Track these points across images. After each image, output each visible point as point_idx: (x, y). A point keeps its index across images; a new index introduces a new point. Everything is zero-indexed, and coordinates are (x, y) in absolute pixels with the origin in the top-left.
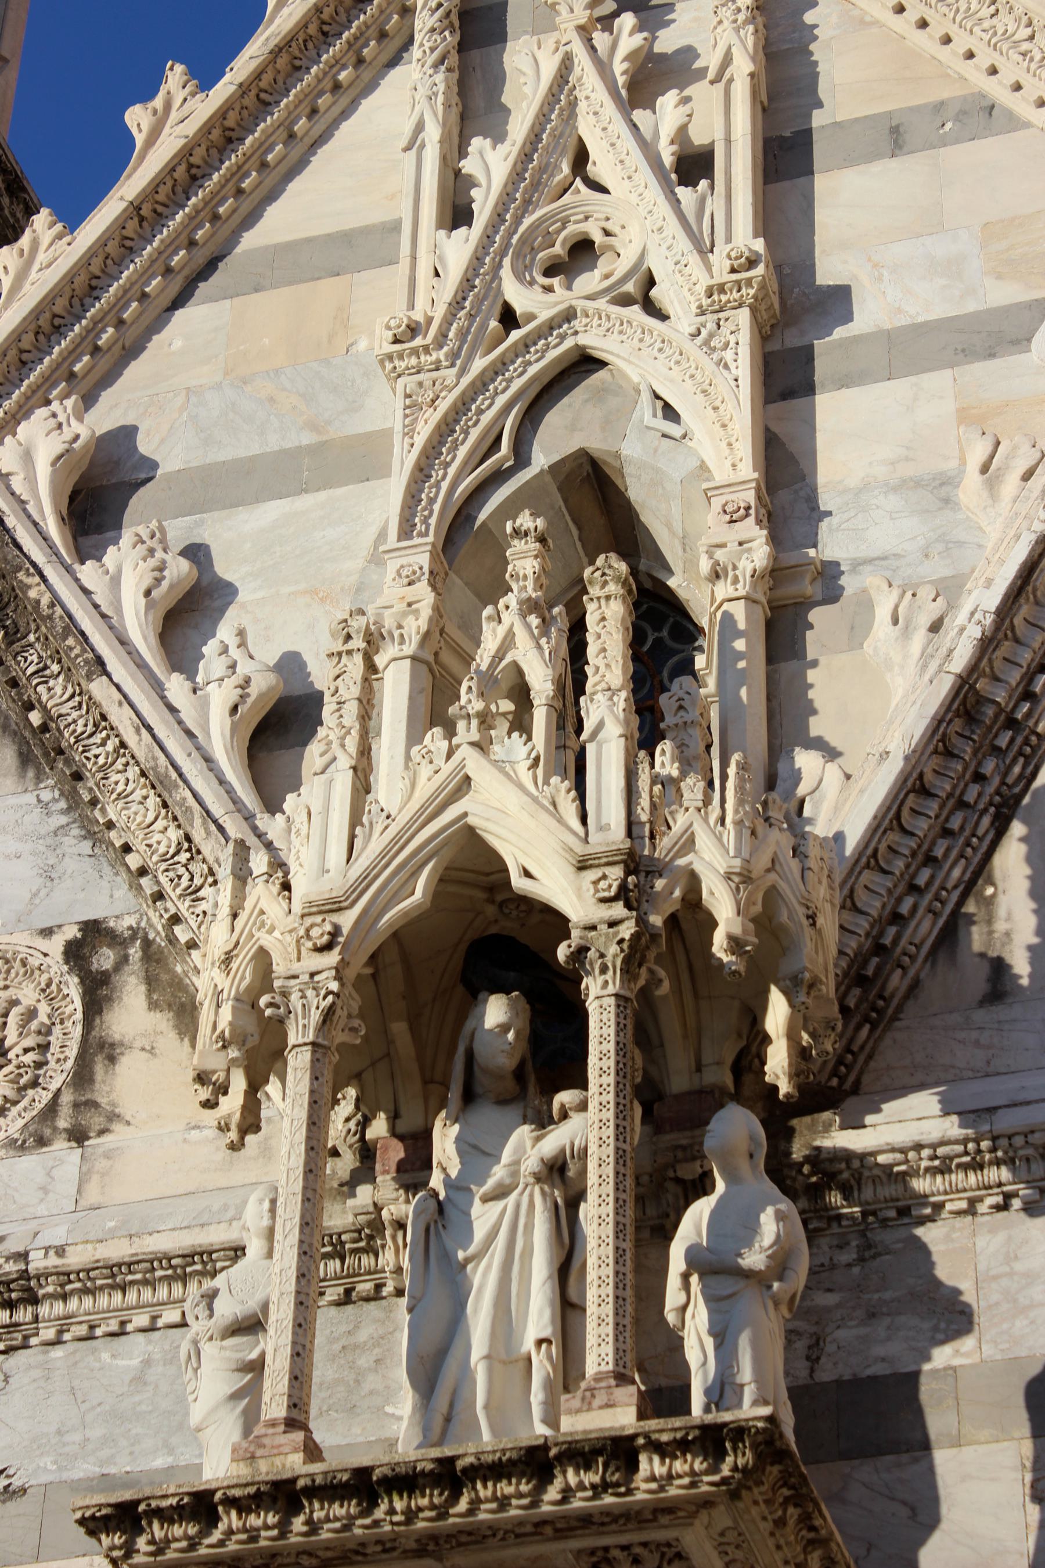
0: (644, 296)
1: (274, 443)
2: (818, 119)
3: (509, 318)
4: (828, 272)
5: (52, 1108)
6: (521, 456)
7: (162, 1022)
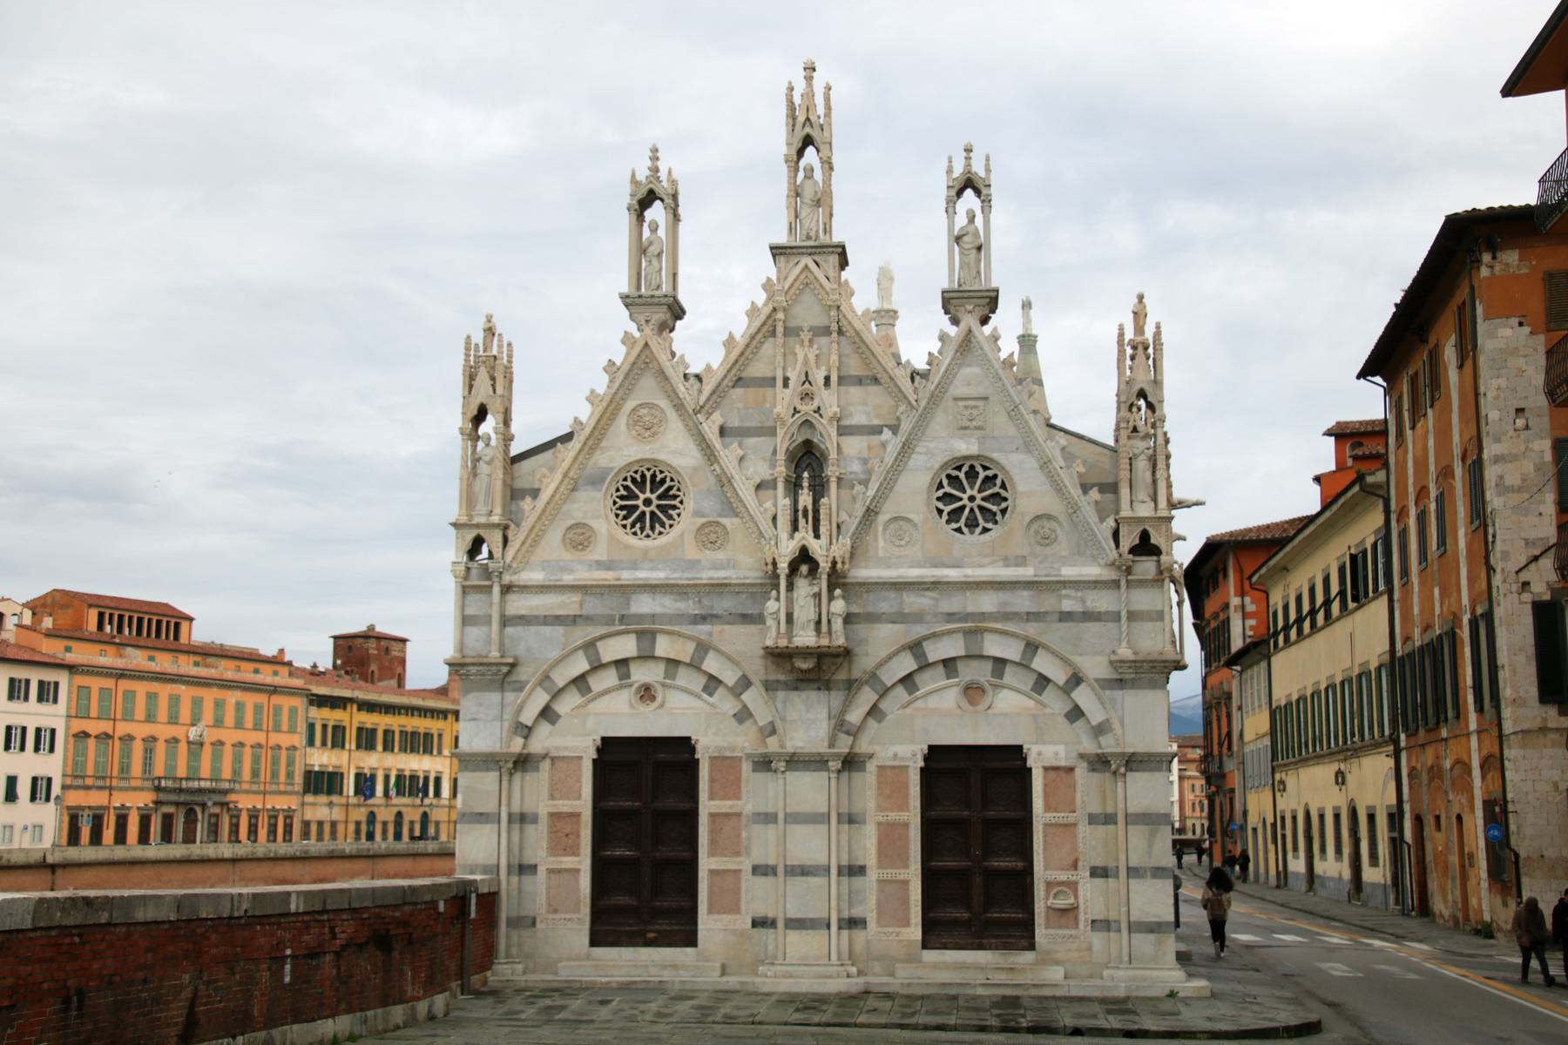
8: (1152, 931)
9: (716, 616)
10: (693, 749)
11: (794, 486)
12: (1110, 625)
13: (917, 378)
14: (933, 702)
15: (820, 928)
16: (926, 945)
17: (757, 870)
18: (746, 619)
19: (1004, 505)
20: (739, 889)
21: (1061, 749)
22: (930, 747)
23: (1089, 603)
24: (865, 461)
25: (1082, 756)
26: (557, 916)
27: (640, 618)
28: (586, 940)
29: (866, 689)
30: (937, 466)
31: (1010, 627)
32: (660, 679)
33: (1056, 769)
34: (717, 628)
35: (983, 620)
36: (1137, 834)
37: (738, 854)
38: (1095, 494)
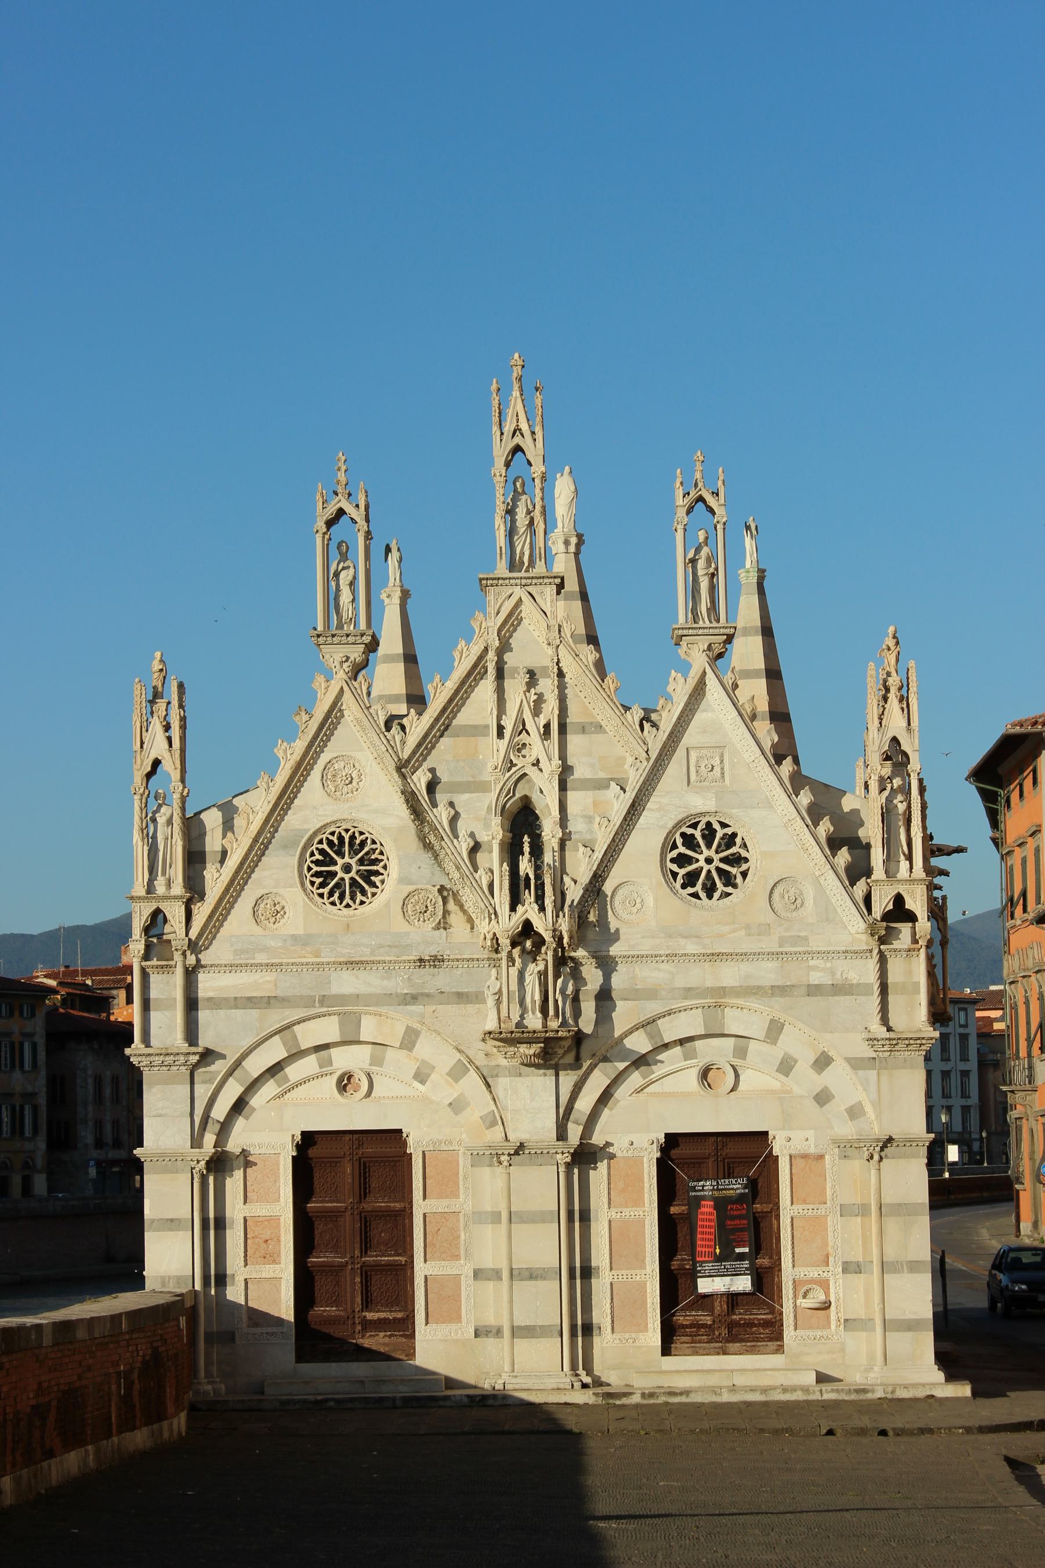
0: (537, 763)
1: (465, 779)
5: (439, 922)
7: (457, 908)
8: (909, 1329)
9: (428, 995)
10: (405, 1144)
11: (512, 852)
12: (863, 998)
13: (646, 725)
14: (668, 1085)
15: (552, 1336)
16: (666, 1351)
17: (477, 1274)
18: (461, 997)
19: (744, 867)
20: (459, 1296)
22: (667, 1135)
23: (838, 976)
24: (590, 819)
25: (834, 1141)
26: (258, 1330)
27: (342, 999)
28: (292, 1356)
29: (596, 1072)
31: (753, 1003)
32: (366, 1066)
33: (805, 1156)
34: (430, 1008)
35: (724, 996)
36: (892, 1225)
37: (457, 1257)
38: (844, 856)
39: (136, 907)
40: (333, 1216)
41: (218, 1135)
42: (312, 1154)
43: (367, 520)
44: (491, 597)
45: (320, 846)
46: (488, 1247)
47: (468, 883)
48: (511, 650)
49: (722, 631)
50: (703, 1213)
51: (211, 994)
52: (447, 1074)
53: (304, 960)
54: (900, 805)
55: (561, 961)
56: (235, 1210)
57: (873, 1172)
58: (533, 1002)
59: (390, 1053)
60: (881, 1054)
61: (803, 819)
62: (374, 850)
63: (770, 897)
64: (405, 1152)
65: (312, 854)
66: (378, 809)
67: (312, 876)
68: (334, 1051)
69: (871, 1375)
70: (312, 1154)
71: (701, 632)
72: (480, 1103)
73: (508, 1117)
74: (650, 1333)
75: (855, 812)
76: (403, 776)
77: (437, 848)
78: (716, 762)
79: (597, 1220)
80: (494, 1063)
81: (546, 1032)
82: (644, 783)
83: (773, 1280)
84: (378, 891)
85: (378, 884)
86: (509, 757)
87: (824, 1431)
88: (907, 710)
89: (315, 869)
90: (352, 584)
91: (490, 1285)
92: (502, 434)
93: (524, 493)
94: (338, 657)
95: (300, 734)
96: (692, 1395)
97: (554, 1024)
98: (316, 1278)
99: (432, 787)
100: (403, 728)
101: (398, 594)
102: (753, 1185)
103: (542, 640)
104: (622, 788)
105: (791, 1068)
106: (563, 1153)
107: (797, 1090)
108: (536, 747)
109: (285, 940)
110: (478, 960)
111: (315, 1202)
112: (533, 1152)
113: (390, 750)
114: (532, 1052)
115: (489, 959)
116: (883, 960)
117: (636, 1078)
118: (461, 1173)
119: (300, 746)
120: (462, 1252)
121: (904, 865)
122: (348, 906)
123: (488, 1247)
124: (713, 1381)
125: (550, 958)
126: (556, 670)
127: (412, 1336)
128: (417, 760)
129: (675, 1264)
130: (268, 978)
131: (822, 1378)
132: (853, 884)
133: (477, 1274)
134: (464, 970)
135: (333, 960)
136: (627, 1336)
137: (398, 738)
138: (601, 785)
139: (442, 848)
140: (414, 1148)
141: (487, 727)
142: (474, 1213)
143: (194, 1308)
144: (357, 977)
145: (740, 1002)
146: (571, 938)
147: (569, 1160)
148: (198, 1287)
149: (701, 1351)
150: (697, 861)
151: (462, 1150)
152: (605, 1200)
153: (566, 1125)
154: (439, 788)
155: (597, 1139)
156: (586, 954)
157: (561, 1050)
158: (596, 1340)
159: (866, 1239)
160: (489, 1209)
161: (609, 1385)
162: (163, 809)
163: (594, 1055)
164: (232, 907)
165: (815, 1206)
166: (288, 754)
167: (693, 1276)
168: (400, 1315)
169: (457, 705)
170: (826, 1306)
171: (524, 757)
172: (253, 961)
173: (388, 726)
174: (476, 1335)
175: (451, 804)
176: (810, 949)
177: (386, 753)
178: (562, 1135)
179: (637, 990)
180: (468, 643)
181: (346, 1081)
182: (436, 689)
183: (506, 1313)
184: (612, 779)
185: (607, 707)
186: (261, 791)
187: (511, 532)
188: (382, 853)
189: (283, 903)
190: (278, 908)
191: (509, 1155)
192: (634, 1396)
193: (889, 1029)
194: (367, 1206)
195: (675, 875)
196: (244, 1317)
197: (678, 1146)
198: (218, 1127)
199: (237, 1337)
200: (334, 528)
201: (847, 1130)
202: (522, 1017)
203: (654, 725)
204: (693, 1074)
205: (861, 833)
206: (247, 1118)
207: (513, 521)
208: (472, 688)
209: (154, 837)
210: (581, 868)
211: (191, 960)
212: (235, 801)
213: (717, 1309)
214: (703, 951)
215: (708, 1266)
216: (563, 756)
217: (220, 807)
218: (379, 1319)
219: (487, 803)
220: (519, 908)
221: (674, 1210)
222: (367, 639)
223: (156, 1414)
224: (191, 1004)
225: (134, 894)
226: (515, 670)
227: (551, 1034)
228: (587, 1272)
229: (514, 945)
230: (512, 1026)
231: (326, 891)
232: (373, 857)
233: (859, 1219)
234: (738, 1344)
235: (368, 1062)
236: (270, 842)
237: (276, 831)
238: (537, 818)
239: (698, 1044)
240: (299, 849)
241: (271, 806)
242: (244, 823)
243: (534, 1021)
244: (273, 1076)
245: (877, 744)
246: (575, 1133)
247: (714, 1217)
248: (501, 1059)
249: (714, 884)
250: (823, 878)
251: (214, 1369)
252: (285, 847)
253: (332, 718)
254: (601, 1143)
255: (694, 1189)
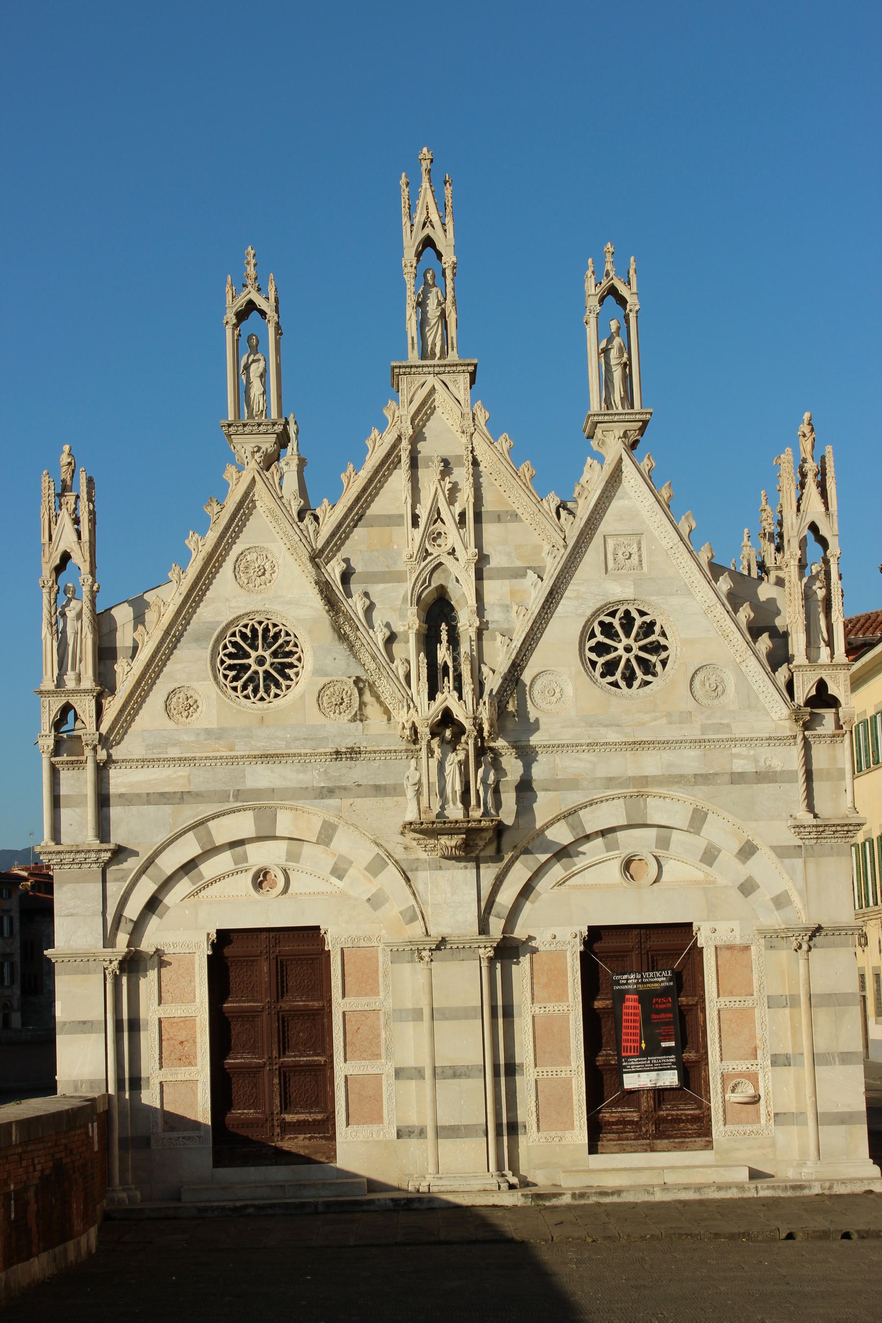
0: (452, 552)
2: (483, 509)
3: (427, 550)
4: (485, 552)
5: (356, 714)
6: (430, 584)
7: (373, 699)
8: (842, 1122)
9: (345, 788)
10: (323, 940)
11: (428, 642)
12: (786, 786)
13: (563, 513)
14: (589, 877)
15: (477, 1136)
16: (593, 1149)
17: (399, 1073)
18: (379, 790)
20: (381, 1095)
21: (735, 925)
22: (590, 928)
23: (762, 764)
24: (507, 608)
25: (760, 932)
26: (175, 1135)
27: (257, 793)
28: (210, 1161)
29: (518, 865)
30: (589, 613)
31: (676, 792)
32: (282, 862)
33: (730, 948)
34: (347, 802)
35: (646, 785)
36: (822, 1016)
37: (377, 1056)
38: (765, 643)
39: (45, 701)
40: (249, 1016)
41: (132, 934)
42: (229, 952)
43: (277, 311)
44: (403, 386)
45: (233, 639)
46: (410, 1045)
47: (385, 673)
48: (425, 439)
49: (638, 417)
50: (628, 1007)
51: (122, 790)
52: (366, 869)
53: (218, 754)
54: (819, 592)
55: (481, 751)
56: (150, 1011)
57: (802, 962)
58: (454, 792)
59: (307, 849)
60: (807, 842)
61: (723, 605)
62: (288, 643)
63: (691, 685)
64: (323, 949)
65: (225, 647)
66: (291, 599)
67: (225, 669)
68: (249, 847)
69: (805, 1170)
70: (229, 952)
71: (616, 418)
72: (399, 898)
73: (429, 911)
74: (577, 1131)
75: (772, 601)
76: (317, 566)
77: (352, 638)
78: (634, 549)
79: (520, 1015)
80: (413, 856)
81: (469, 822)
82: (562, 571)
83: (700, 1074)
84: (293, 683)
85: (293, 676)
86: (424, 546)
87: (784, 1235)
88: (824, 494)
89: (229, 662)
90: (263, 376)
91: (413, 1084)
92: (412, 225)
93: (434, 285)
94: (249, 448)
95: (212, 525)
96: (624, 1194)
97: (476, 814)
98: (233, 1080)
99: (346, 577)
100: (316, 518)
101: (296, 461)
102: (677, 977)
103: (456, 428)
104: (539, 577)
105: (715, 858)
106: (485, 947)
107: (721, 881)
108: (452, 535)
109: (198, 734)
110: (395, 751)
111: (232, 1002)
112: (455, 946)
113: (304, 540)
114: (453, 843)
115: (407, 751)
116: (807, 746)
117: (557, 871)
118: (381, 970)
119: (212, 536)
120: (383, 1051)
121: (825, 651)
122: (262, 699)
123: (410, 1045)
124: (644, 1179)
125: (471, 748)
126: (470, 458)
127: (333, 1138)
128: (331, 550)
129: (600, 1060)
130: (181, 773)
131: (755, 1175)
132: (774, 670)
133: (399, 1073)
134: (381, 762)
135: (247, 753)
136: (553, 1134)
137: (311, 528)
138: (519, 574)
139: (358, 638)
140: (332, 945)
141: (401, 516)
142: (394, 1010)
143: (108, 1113)
144: (272, 771)
145: (663, 791)
146: (491, 726)
147: (491, 954)
148: (111, 1091)
149: (628, 1148)
150: (616, 649)
151: (382, 946)
152: (528, 995)
153: (488, 919)
154: (353, 578)
155: (520, 933)
156: (506, 744)
157: (482, 843)
158: (522, 1139)
159: (795, 1031)
160: (410, 1006)
161: (535, 1185)
162: (73, 603)
163: (515, 847)
164: (144, 701)
165: (742, 998)
166: (200, 546)
167: (619, 1071)
168: (319, 1117)
169: (370, 494)
170: (755, 1100)
171: (439, 546)
172: (166, 756)
173: (301, 515)
174: (399, 1136)
175: (366, 595)
176: (733, 736)
177: (300, 543)
178: (484, 929)
179: (559, 780)
180: (381, 431)
181: (261, 878)
182: (349, 478)
183: (429, 1112)
184: (529, 568)
185: (523, 494)
186: (174, 584)
187: (423, 324)
188: (296, 645)
189: (196, 697)
190: (191, 701)
191: (431, 950)
192: (564, 1197)
193: (816, 816)
194: (284, 1005)
195: (594, 664)
196: (160, 1121)
197: (601, 939)
198: (131, 926)
199: (153, 1142)
200: (244, 323)
201: (774, 920)
202: (443, 808)
203: (571, 512)
204: (615, 867)
205: (778, 622)
206: (161, 917)
207: (424, 313)
208: (386, 477)
209: (64, 631)
210: (499, 657)
211: (102, 755)
212: (147, 597)
213: (644, 1106)
214: (624, 740)
215: (634, 1062)
216: (479, 545)
217: (131, 603)
218: (298, 1121)
219: (402, 593)
220: (439, 697)
221: (598, 1004)
222: (279, 428)
223: (58, 1233)
224: (103, 801)
225: (43, 688)
226: (430, 459)
227: (473, 825)
228: (511, 1069)
229: (433, 735)
230: (432, 816)
231: (239, 684)
232: (287, 649)
233: (787, 1011)
234: (666, 1141)
235: (284, 858)
236: (182, 635)
237: (188, 623)
238: (452, 609)
239: (620, 834)
240: (212, 642)
241: (182, 597)
242: (156, 615)
243: (455, 812)
244: (187, 874)
245: (796, 529)
246: (496, 926)
247: (639, 1011)
248: (420, 852)
249: (633, 673)
250: (744, 664)
251: (130, 1175)
252: (198, 639)
253: (244, 509)
254: (523, 937)
255: (617, 983)
